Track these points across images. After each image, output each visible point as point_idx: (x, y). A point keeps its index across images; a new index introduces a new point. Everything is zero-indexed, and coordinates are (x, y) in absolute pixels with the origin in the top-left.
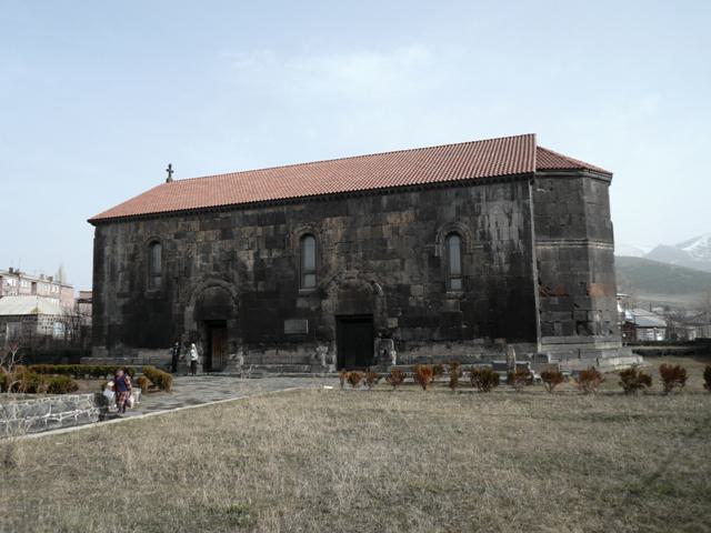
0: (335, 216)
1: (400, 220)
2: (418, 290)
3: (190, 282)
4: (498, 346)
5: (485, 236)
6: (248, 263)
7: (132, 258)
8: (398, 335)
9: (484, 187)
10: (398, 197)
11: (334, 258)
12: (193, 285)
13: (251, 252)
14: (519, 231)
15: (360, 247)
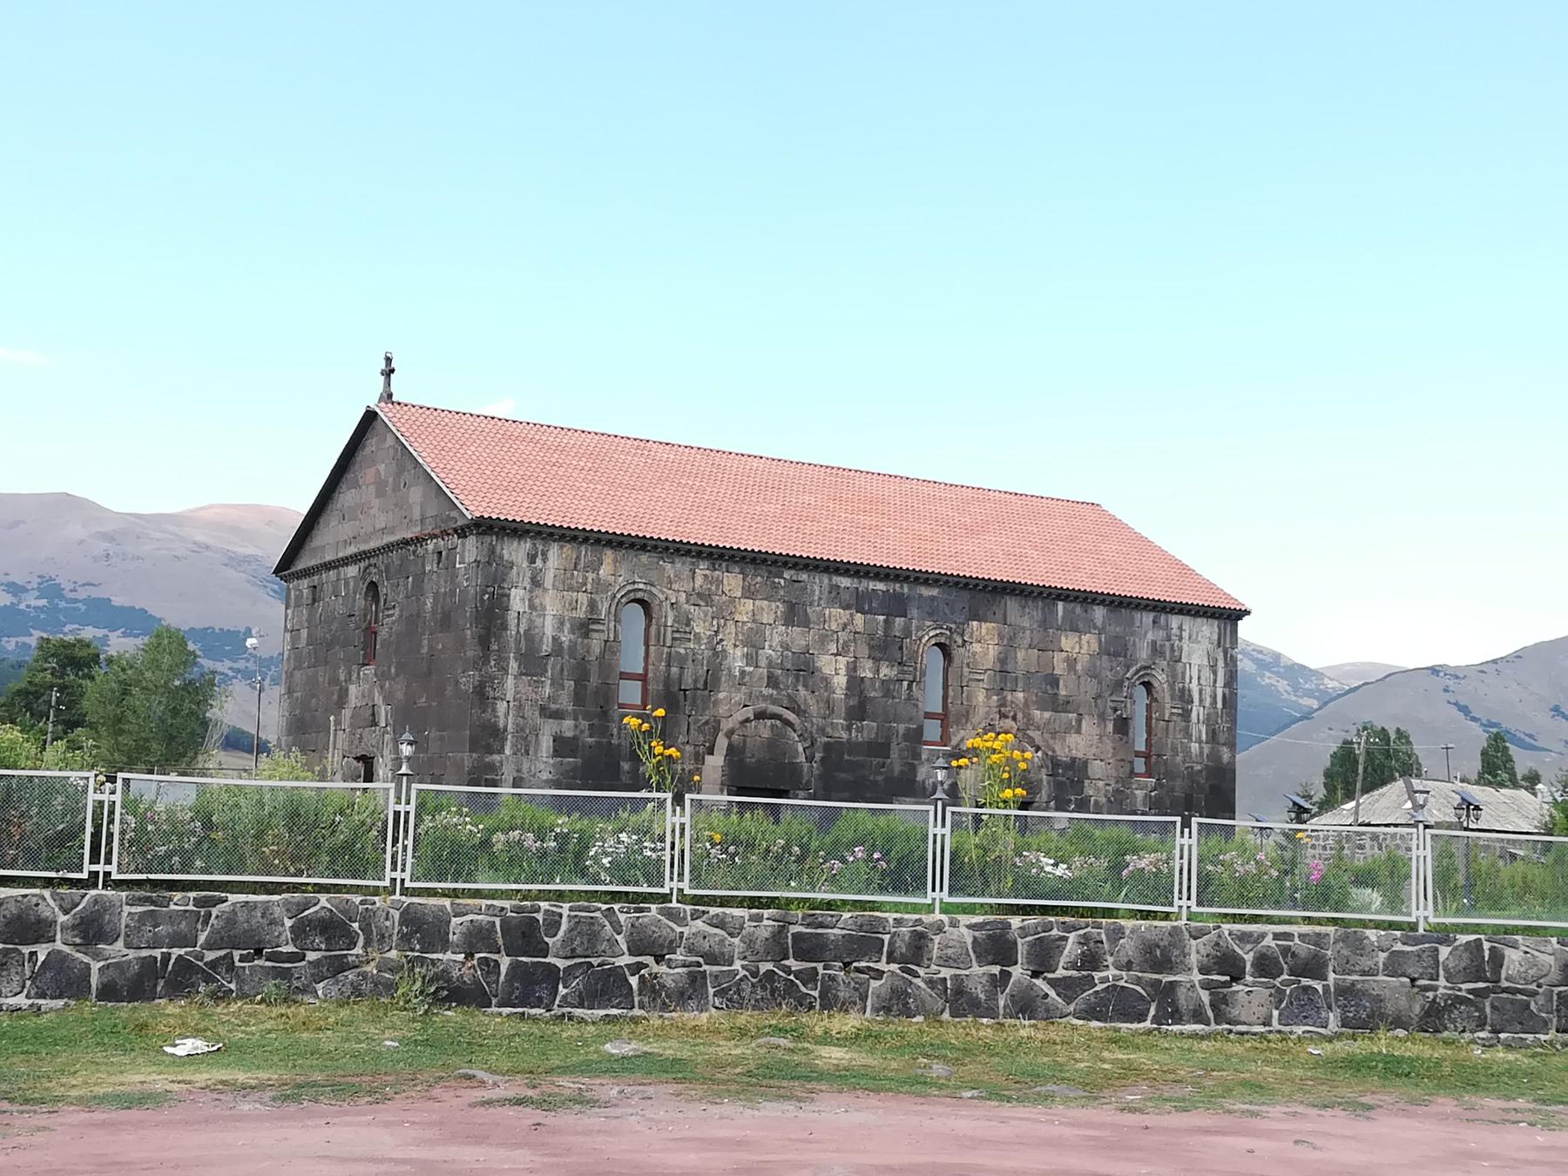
0: (985, 622)
1: (1079, 646)
2: (1096, 768)
3: (716, 703)
5: (1184, 697)
6: (835, 680)
7: (584, 628)
10: (1078, 609)
12: (722, 710)
14: (1224, 695)
15: (1020, 684)
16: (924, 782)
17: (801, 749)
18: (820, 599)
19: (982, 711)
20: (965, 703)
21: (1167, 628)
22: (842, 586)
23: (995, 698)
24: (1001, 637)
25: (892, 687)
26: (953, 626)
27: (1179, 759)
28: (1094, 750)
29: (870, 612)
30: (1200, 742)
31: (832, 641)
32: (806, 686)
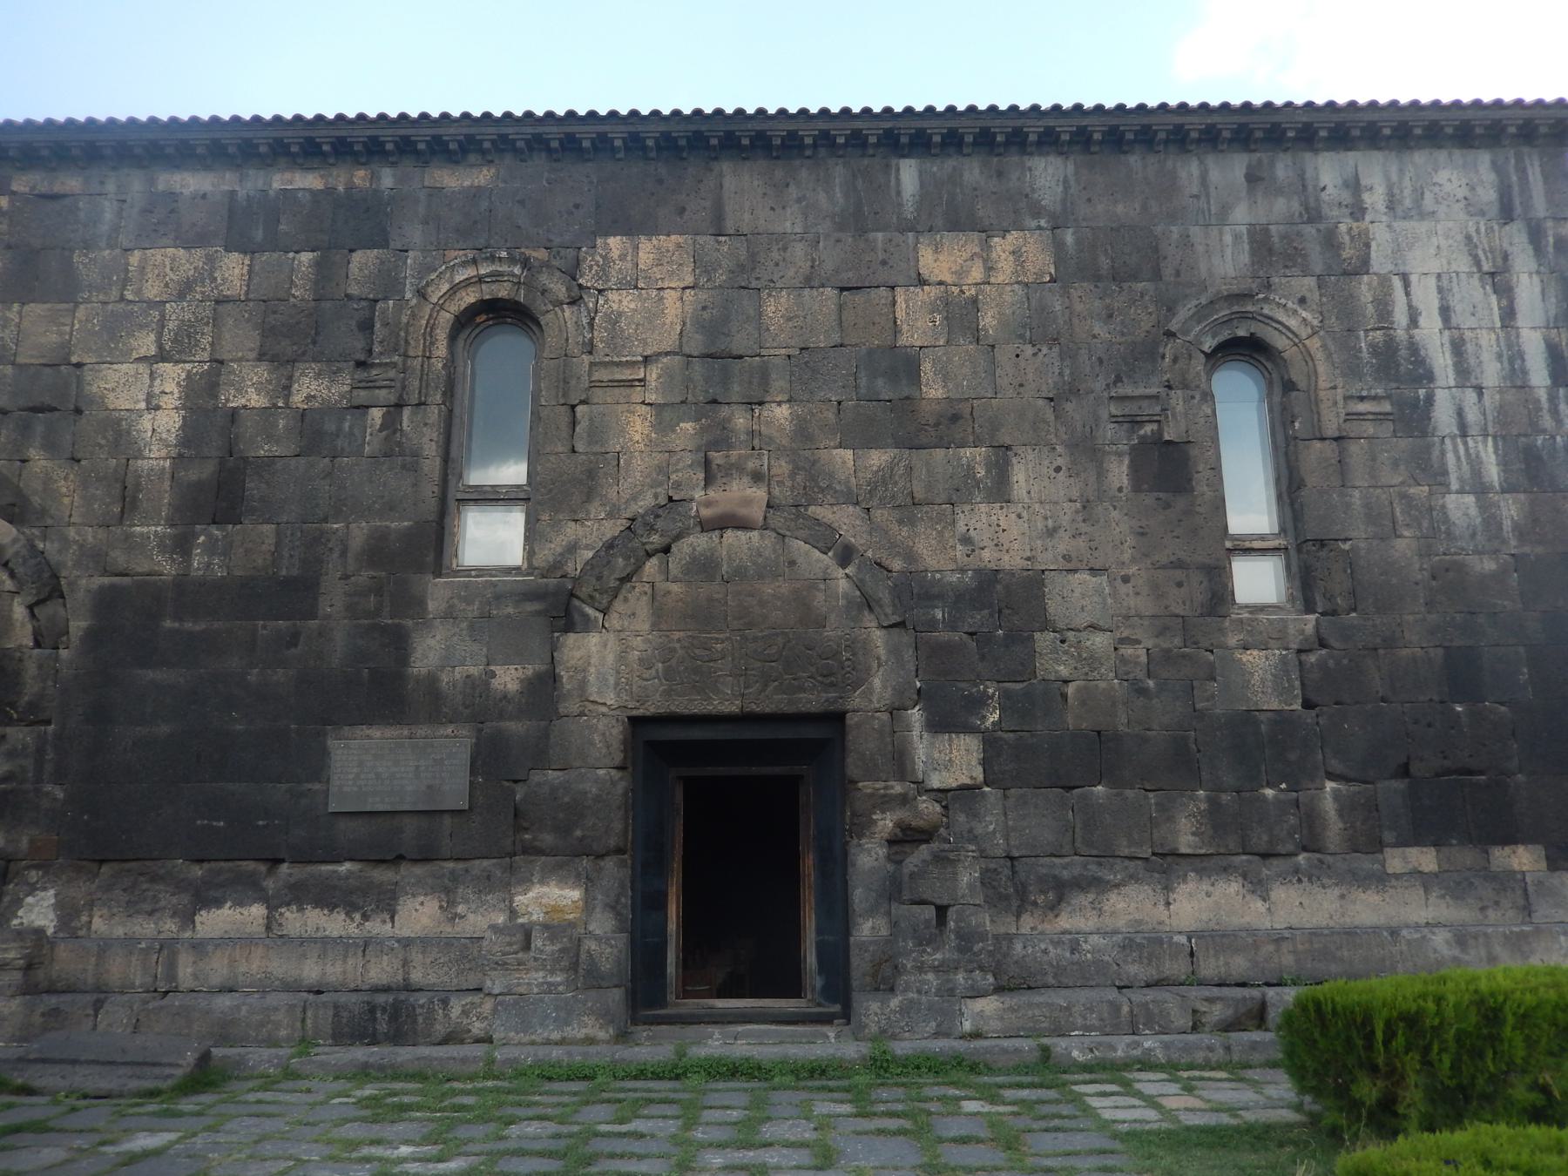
0: (652, 230)
4: (1507, 881)
6: (146, 423)
8: (990, 822)
9: (1377, 157)
10: (972, 171)
11: (638, 427)
13: (172, 377)
15: (778, 383)
16: (432, 680)
17: (19, 611)
18: (116, 229)
19: (639, 466)
20: (580, 447)
21: (1303, 187)
22: (186, 192)
23: (688, 426)
24: (703, 266)
25: (330, 427)
26: (542, 254)
27: (1404, 545)
28: (1063, 544)
29: (273, 243)
30: (1479, 488)
31: (141, 327)
32: (51, 447)
